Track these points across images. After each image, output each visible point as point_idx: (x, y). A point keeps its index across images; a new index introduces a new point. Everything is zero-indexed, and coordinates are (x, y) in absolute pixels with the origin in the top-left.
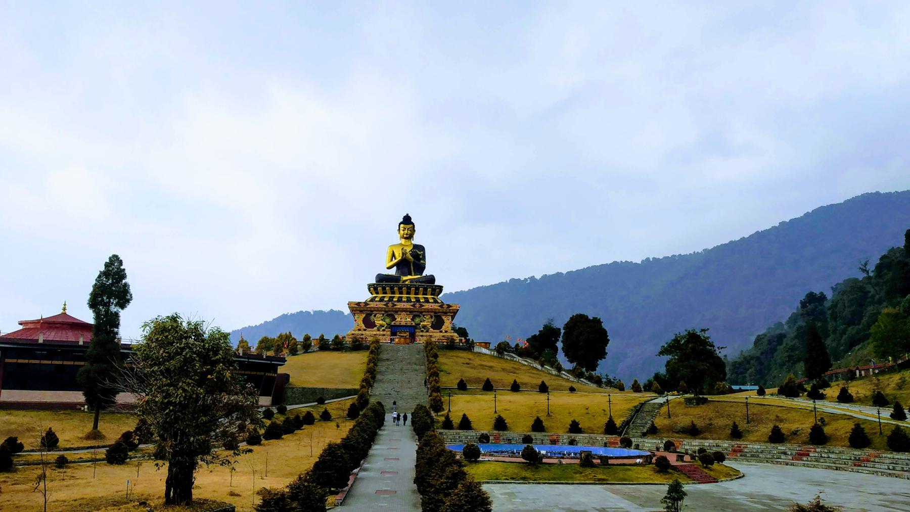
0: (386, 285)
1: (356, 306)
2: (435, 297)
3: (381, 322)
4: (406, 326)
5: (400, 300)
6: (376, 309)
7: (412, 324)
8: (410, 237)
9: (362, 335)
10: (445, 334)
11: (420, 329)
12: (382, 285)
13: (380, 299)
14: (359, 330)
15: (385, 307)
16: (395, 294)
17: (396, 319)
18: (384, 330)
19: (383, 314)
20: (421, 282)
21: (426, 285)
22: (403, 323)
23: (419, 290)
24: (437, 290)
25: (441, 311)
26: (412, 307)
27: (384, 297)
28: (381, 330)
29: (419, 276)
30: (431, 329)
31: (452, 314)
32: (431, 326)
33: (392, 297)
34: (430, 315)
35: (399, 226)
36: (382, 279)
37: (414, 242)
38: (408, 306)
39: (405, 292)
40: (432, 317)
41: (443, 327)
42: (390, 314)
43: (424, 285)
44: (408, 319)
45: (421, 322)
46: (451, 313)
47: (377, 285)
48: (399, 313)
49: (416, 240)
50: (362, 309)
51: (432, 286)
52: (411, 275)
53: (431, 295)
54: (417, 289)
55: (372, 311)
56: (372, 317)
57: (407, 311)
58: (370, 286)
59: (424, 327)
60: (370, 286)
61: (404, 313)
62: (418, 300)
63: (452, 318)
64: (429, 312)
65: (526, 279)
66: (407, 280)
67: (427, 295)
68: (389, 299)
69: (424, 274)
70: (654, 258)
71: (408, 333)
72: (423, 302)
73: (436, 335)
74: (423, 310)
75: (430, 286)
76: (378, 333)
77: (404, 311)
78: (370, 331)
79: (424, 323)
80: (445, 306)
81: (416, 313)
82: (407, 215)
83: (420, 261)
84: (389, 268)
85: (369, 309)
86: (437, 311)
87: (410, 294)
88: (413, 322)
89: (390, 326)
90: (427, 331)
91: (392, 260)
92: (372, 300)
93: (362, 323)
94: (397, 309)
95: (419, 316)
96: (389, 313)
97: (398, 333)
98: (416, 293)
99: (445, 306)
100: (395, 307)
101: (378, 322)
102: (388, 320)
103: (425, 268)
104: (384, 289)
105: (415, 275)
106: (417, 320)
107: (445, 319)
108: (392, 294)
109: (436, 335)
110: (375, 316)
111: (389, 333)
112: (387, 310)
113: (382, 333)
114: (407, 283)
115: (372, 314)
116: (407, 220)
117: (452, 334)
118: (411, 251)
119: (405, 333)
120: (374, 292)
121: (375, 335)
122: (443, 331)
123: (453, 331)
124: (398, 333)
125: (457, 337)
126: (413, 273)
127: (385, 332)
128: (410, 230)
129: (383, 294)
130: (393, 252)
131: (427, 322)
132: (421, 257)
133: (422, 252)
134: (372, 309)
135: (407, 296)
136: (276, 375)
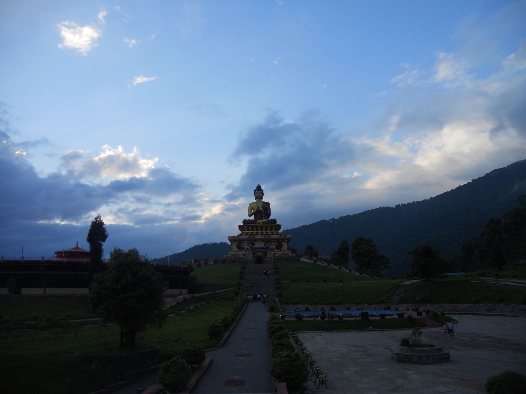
1: (232, 238)
2: (277, 231)
3: (247, 247)
4: (261, 248)
5: (257, 234)
9: (237, 254)
14: (235, 252)
16: (254, 231)
17: (255, 245)
18: (249, 251)
19: (248, 242)
20: (269, 223)
26: (264, 238)
27: (248, 232)
29: (267, 220)
30: (276, 250)
31: (287, 241)
35: (255, 191)
36: (245, 222)
39: (259, 229)
40: (276, 243)
42: (252, 242)
43: (270, 225)
44: (262, 244)
45: (270, 246)
49: (265, 200)
51: (275, 225)
52: (262, 219)
53: (275, 230)
54: (267, 227)
58: (240, 227)
59: (272, 248)
60: (240, 227)
62: (267, 233)
63: (287, 243)
65: (330, 220)
67: (272, 230)
69: (270, 218)
70: (402, 204)
72: (270, 234)
73: (279, 253)
75: (274, 225)
76: (246, 253)
78: (241, 252)
79: (272, 246)
80: (283, 236)
81: (267, 241)
82: (259, 185)
83: (267, 211)
84: (250, 216)
89: (252, 249)
90: (273, 251)
92: (241, 234)
95: (268, 242)
96: (251, 241)
99: (283, 236)
101: (246, 247)
102: (251, 246)
103: (270, 215)
105: (265, 219)
106: (268, 245)
109: (279, 253)
110: (243, 243)
111: (252, 253)
113: (248, 253)
115: (241, 242)
116: (259, 188)
117: (288, 252)
119: (261, 252)
122: (283, 250)
123: (288, 250)
125: (291, 254)
126: (264, 218)
130: (252, 206)
131: (273, 246)
132: (268, 209)
133: (268, 206)
135: (261, 231)
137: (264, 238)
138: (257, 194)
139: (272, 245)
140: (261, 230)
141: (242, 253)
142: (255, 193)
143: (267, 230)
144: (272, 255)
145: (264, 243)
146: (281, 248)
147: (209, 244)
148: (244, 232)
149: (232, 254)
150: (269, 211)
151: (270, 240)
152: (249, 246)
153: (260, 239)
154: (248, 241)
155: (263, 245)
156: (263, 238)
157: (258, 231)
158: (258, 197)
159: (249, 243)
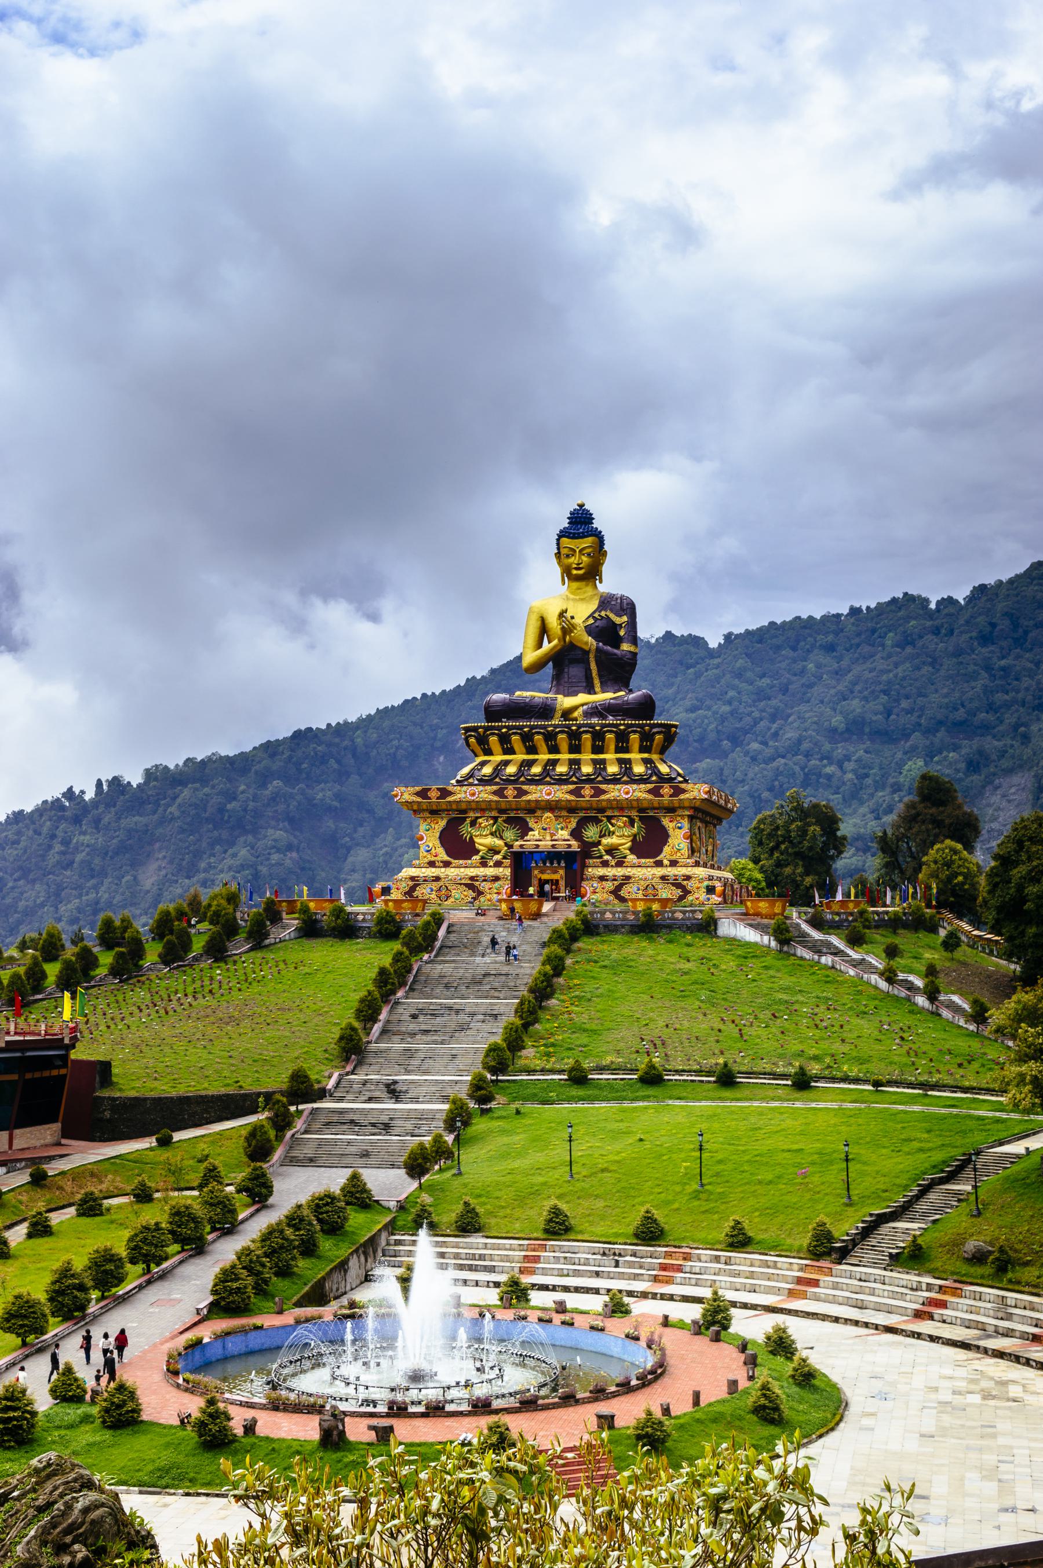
0: (509, 728)
2: (655, 757)
3: (490, 841)
5: (547, 777)
6: (474, 805)
7: (570, 846)
8: (592, 574)
9: (437, 879)
10: (671, 871)
11: (601, 857)
12: (499, 728)
13: (495, 769)
14: (432, 864)
16: (537, 753)
18: (498, 864)
19: (495, 819)
21: (623, 723)
22: (546, 844)
23: (603, 740)
24: (657, 737)
25: (656, 805)
26: (572, 798)
28: (491, 863)
29: (609, 695)
30: (632, 858)
32: (631, 849)
33: (528, 760)
35: (558, 540)
37: (604, 587)
38: (560, 793)
40: (632, 823)
41: (667, 849)
43: (617, 726)
45: (604, 835)
47: (486, 729)
48: (539, 813)
49: (610, 583)
50: (434, 808)
51: (642, 726)
54: (598, 737)
55: (464, 812)
56: (466, 829)
57: (561, 809)
59: (611, 851)
66: (576, 708)
67: (627, 751)
68: (519, 770)
71: (562, 872)
73: (643, 872)
74: (604, 804)
76: (481, 871)
79: (613, 840)
82: (581, 506)
83: (618, 647)
85: (454, 807)
86: (645, 805)
87: (580, 752)
88: (573, 843)
90: (620, 864)
91: (540, 645)
93: (438, 843)
94: (533, 805)
95: (596, 821)
97: (536, 872)
98: (597, 749)
101: (484, 841)
102: (509, 835)
104: (504, 739)
106: (591, 833)
107: (671, 825)
108: (528, 753)
110: (473, 823)
111: (508, 872)
112: (503, 806)
113: (490, 871)
114: (575, 714)
115: (464, 819)
118: (591, 616)
119: (556, 872)
120: (478, 749)
121: (472, 878)
122: (666, 862)
124: (536, 872)
127: (501, 869)
128: (589, 555)
129: (505, 754)
130: (543, 620)
132: (622, 633)
133: (625, 618)
134: (464, 806)
136: (63, 1071)
138: (568, 556)
139: (611, 834)
140: (570, 753)
141: (462, 870)
142: (558, 549)
144: (609, 885)
145: (573, 825)
146: (661, 851)
149: (412, 878)
150: (626, 647)
151: (602, 810)
152: (501, 838)
153: (552, 807)
154: (494, 814)
155: (564, 834)
157: (557, 756)
158: (575, 572)
159: (500, 820)
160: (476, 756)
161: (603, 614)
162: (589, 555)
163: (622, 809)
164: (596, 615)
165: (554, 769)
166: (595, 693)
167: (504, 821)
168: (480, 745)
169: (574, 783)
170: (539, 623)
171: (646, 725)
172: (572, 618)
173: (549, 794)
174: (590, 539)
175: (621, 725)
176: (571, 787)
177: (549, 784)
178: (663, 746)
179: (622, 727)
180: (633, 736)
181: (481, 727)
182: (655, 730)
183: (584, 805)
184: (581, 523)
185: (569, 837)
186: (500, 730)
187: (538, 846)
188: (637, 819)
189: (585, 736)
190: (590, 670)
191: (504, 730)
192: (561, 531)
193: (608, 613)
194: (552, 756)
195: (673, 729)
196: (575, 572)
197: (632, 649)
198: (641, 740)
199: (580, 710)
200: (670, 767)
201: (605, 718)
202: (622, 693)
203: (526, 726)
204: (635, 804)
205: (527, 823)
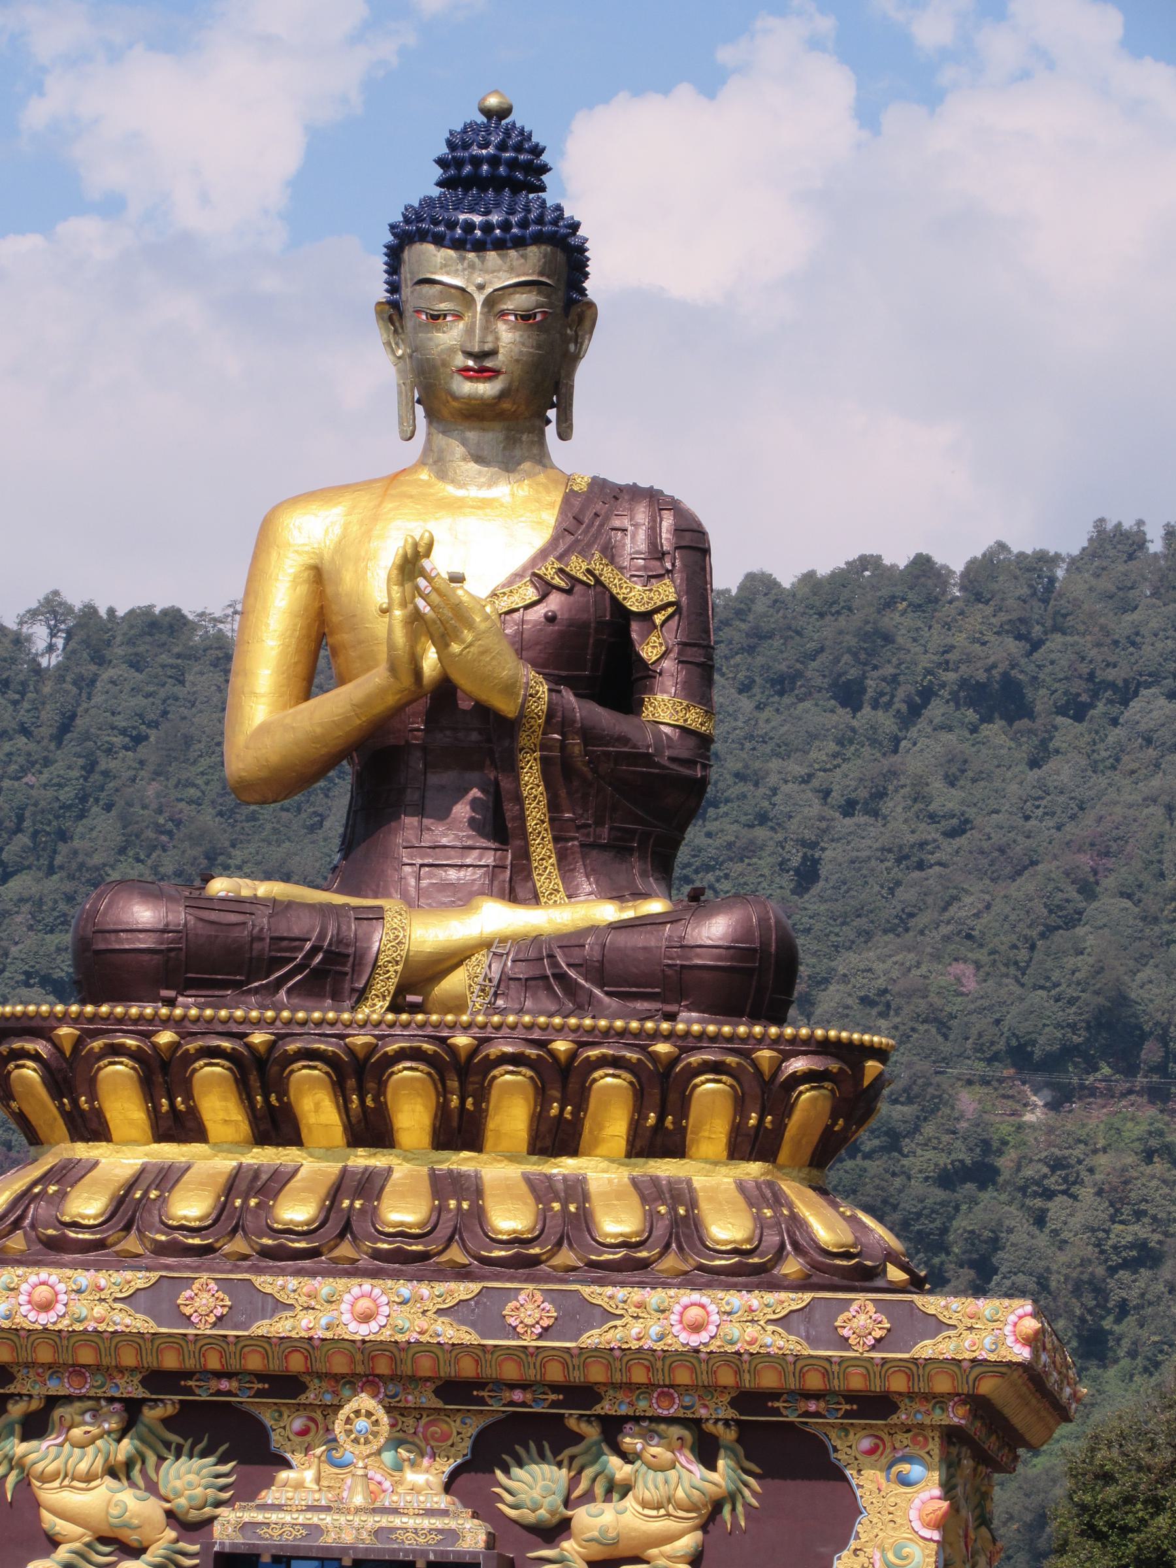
7: (453, 1535)
12: (145, 1028)
15: (141, 1323)
19: (132, 1410)
23: (580, 1097)
25: (814, 1382)
31: (956, 1416)
33: (256, 1173)
34: (694, 1424)
35: (395, 257)
45: (588, 1497)
46: (939, 1400)
51: (744, 1048)
61: (365, 1401)
64: (668, 1390)
68: (222, 1210)
77: (369, 1381)
86: (769, 1380)
100: (262, 1328)
112: (170, 1362)
114: (455, 982)
126: (542, 849)
128: (525, 317)
129: (161, 1136)
132: (650, 651)
137: (467, 1336)
139: (617, 1490)
142: (394, 288)
143: (574, 1152)
145: (465, 1447)
147: (19, 641)
148: (82, 1151)
152: (152, 1488)
156: (449, 1332)
159: (151, 1414)
160: (34, 1139)
161: (577, 566)
162: (525, 317)
163: (668, 1390)
164: (549, 570)
165: (372, 1213)
166: (535, 899)
167: (167, 1422)
168: (53, 1099)
169: (462, 1273)
170: (303, 589)
171: (761, 1041)
172: (457, 579)
173: (366, 1318)
174: (533, 251)
175: (656, 1036)
176: (465, 1290)
177: (353, 1271)
178: (828, 1132)
179: (662, 1048)
180: (708, 1087)
181: (64, 1019)
182: (798, 1065)
183: (510, 1372)
184: (496, 183)
185: (443, 1501)
186: (147, 1035)
187: (315, 1530)
188: (729, 1435)
189: (506, 1077)
190: (519, 799)
191: (165, 1037)
192: (413, 216)
193: (597, 568)
194: (362, 1159)
195: (872, 1067)
196: (467, 388)
197: (694, 719)
198: (740, 1105)
199: (480, 965)
200: (852, 1220)
201: (581, 1003)
202: (656, 906)
203: (259, 1023)
204: (726, 1378)
205: (261, 1433)
